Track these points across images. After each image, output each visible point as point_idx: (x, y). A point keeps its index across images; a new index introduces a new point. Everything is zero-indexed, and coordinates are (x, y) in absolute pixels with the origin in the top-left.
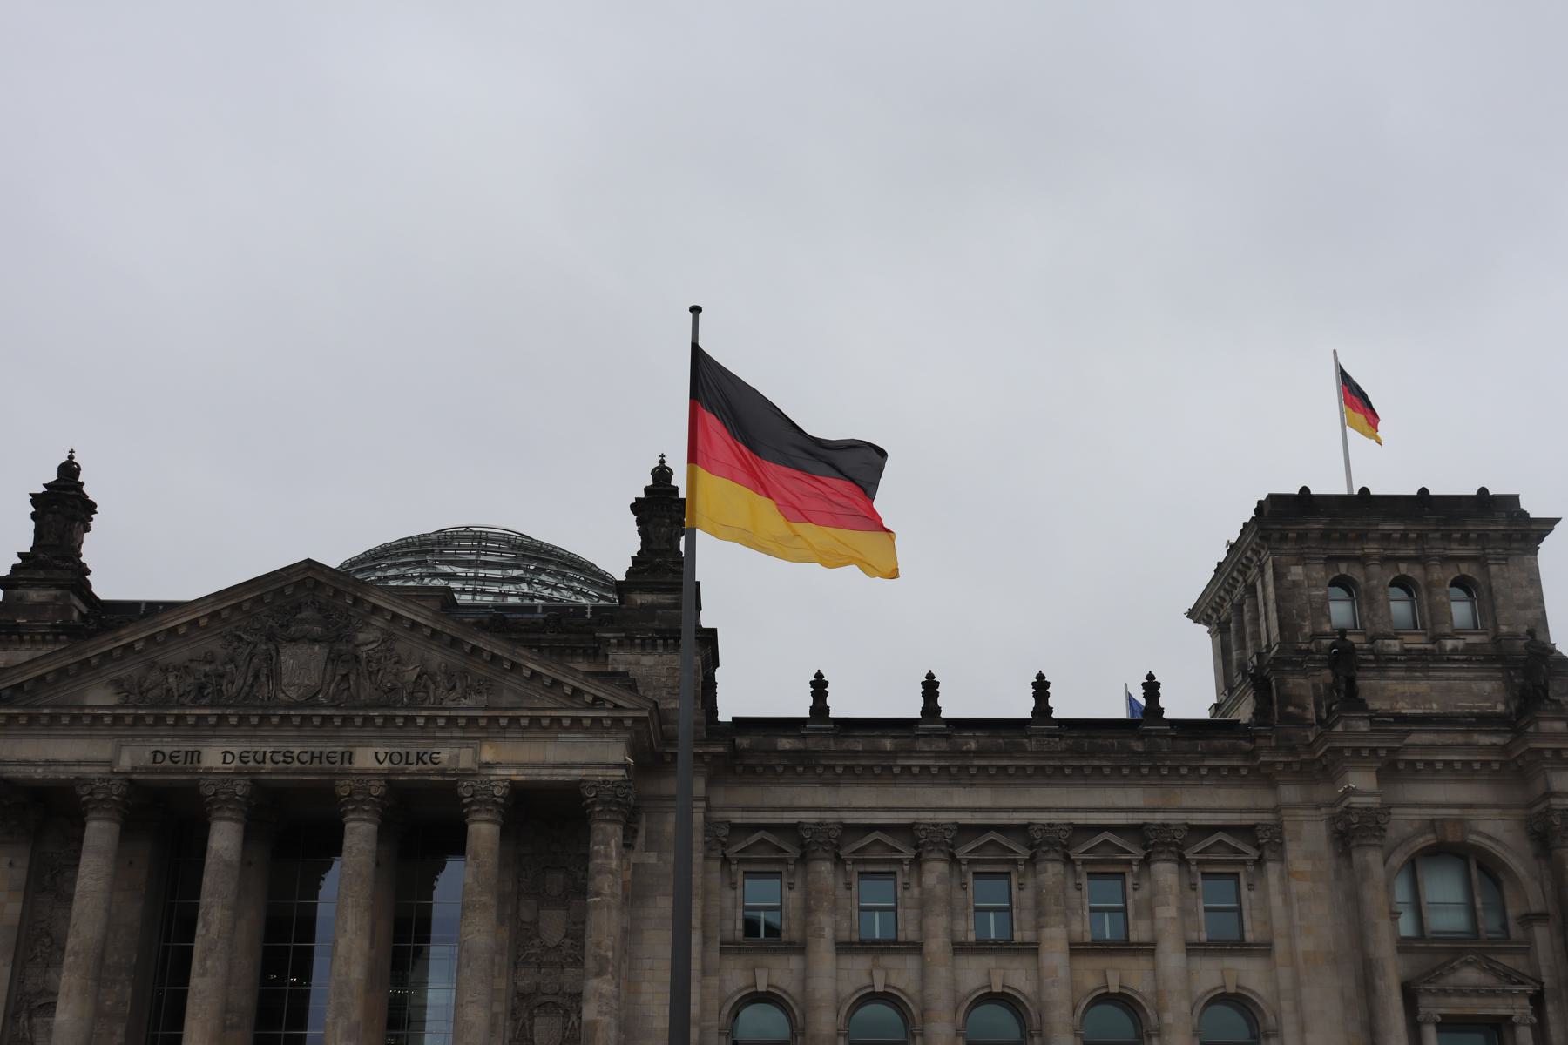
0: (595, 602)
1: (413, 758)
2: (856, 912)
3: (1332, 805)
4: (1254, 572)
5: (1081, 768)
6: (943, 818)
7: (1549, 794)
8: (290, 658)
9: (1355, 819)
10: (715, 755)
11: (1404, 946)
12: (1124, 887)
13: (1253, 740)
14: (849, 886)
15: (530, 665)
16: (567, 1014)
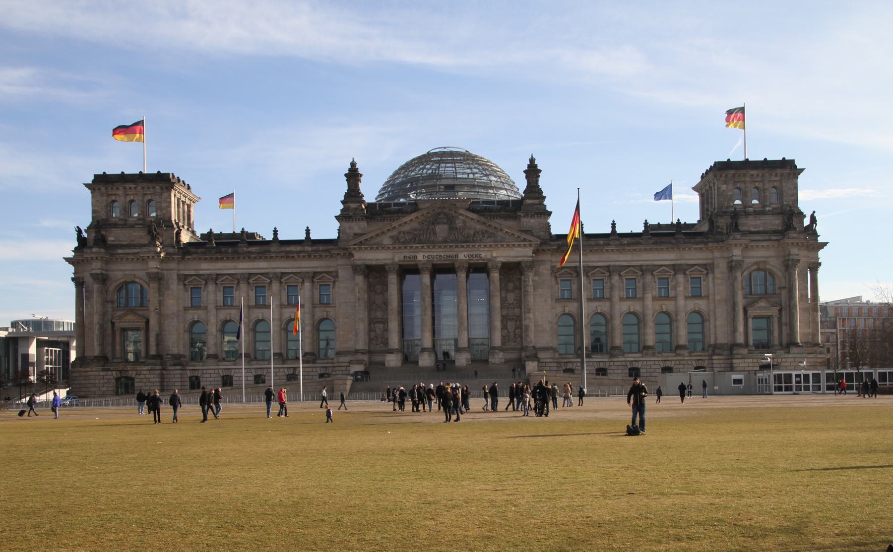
0: (513, 198)
1: (474, 256)
2: (592, 290)
3: (728, 258)
4: (712, 185)
5: (657, 249)
6: (617, 264)
7: (789, 255)
8: (438, 228)
9: (734, 264)
10: (554, 249)
11: (744, 298)
12: (668, 282)
13: (707, 239)
14: (590, 283)
15: (506, 230)
16: (516, 321)
